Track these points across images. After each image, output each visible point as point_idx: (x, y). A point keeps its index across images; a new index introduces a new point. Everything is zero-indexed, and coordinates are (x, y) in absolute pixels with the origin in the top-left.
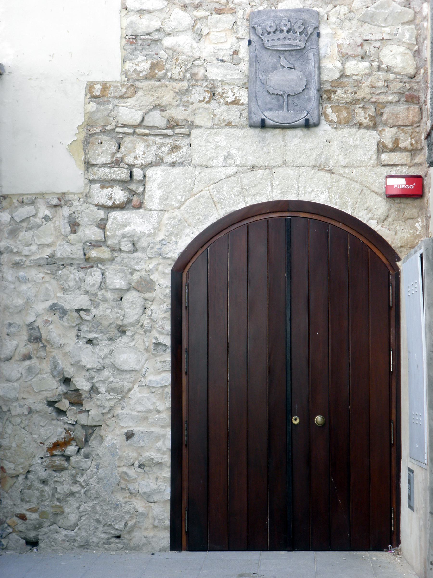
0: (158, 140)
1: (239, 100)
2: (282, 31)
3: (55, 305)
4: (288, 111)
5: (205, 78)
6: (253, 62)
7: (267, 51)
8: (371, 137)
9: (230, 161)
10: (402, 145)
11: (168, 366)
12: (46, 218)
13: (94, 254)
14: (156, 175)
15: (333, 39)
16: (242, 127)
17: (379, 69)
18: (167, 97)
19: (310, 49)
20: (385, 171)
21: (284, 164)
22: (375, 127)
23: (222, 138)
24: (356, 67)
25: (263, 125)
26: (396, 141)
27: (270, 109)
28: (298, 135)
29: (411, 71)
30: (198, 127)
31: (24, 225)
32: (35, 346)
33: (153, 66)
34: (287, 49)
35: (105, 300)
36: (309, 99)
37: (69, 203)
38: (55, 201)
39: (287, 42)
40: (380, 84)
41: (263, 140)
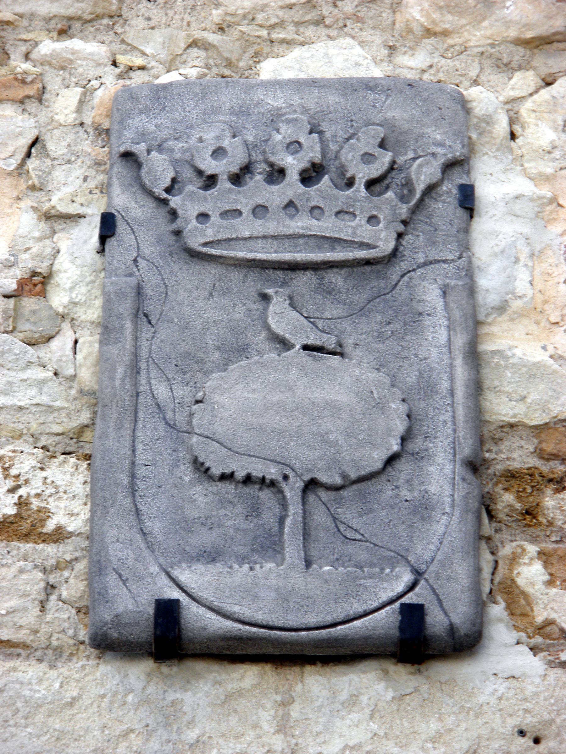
1: (44, 513)
2: (277, 174)
4: (308, 564)
6: (120, 317)
7: (197, 267)
19: (426, 264)
25: (167, 640)
27: (211, 556)
28: (364, 699)
34: (301, 256)
36: (423, 509)
39: (301, 224)
41: (167, 725)
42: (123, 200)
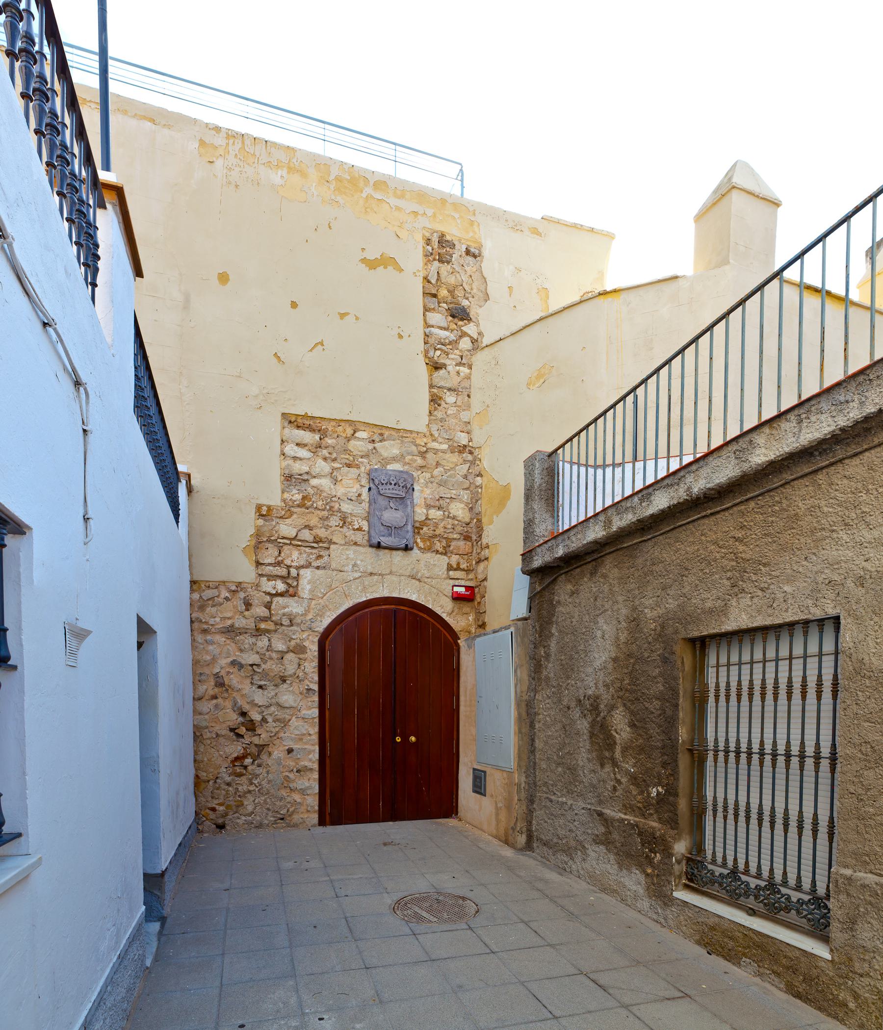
0: (307, 550)
2: (391, 484)
3: (234, 660)
5: (339, 511)
8: (444, 560)
9: (356, 568)
10: (461, 567)
11: (316, 704)
12: (227, 599)
13: (263, 626)
14: (306, 574)
15: (422, 493)
16: (364, 546)
17: (448, 517)
18: (314, 521)
20: (452, 582)
21: (391, 573)
22: (445, 554)
23: (351, 552)
24: (435, 514)
25: (379, 546)
26: (458, 564)
29: (467, 520)
30: (335, 543)
31: (210, 602)
32: (220, 689)
33: (304, 498)
35: (271, 658)
37: (244, 590)
38: (234, 588)
40: (450, 526)
42: (372, 485)
